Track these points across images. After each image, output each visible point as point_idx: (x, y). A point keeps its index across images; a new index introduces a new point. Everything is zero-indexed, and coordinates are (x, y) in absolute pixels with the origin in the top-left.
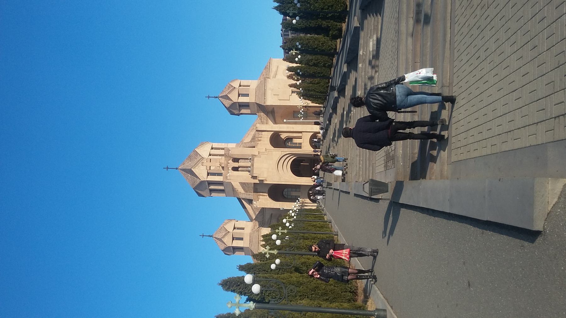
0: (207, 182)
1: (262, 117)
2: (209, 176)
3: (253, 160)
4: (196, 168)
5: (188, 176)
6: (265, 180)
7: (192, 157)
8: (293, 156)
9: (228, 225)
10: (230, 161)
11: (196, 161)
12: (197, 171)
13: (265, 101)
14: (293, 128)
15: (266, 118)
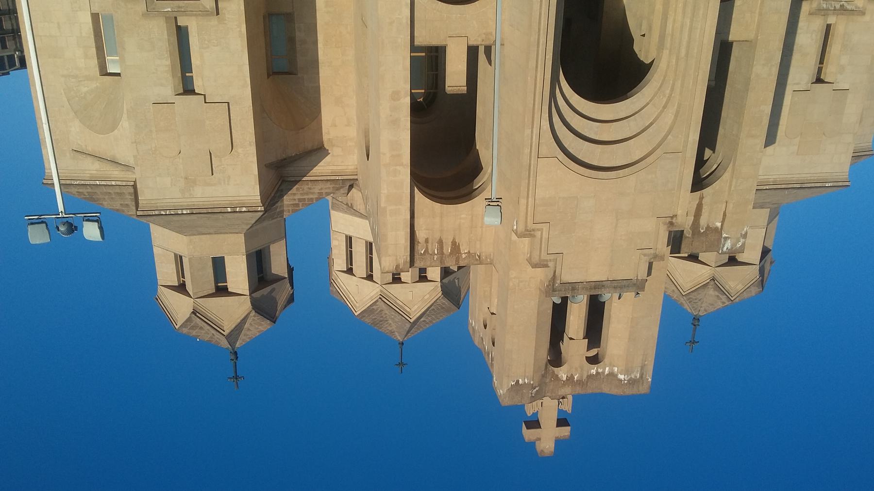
0: (444, 281)
1: (300, 200)
2: (426, 277)
3: (573, 289)
4: (408, 310)
5: (424, 321)
6: (671, 223)
7: (375, 319)
8: (558, 90)
9: (681, 281)
10: (562, 373)
11: (387, 311)
12: (416, 307)
13: (244, 209)
14: (395, 96)
15: (306, 187)
